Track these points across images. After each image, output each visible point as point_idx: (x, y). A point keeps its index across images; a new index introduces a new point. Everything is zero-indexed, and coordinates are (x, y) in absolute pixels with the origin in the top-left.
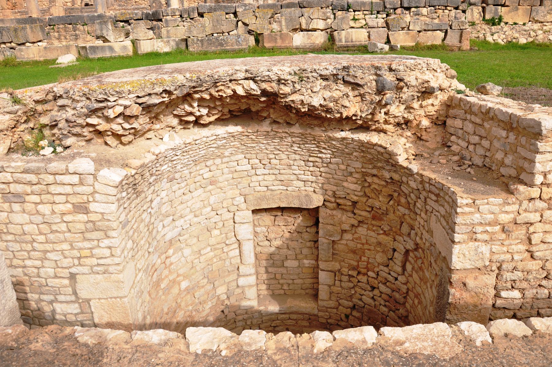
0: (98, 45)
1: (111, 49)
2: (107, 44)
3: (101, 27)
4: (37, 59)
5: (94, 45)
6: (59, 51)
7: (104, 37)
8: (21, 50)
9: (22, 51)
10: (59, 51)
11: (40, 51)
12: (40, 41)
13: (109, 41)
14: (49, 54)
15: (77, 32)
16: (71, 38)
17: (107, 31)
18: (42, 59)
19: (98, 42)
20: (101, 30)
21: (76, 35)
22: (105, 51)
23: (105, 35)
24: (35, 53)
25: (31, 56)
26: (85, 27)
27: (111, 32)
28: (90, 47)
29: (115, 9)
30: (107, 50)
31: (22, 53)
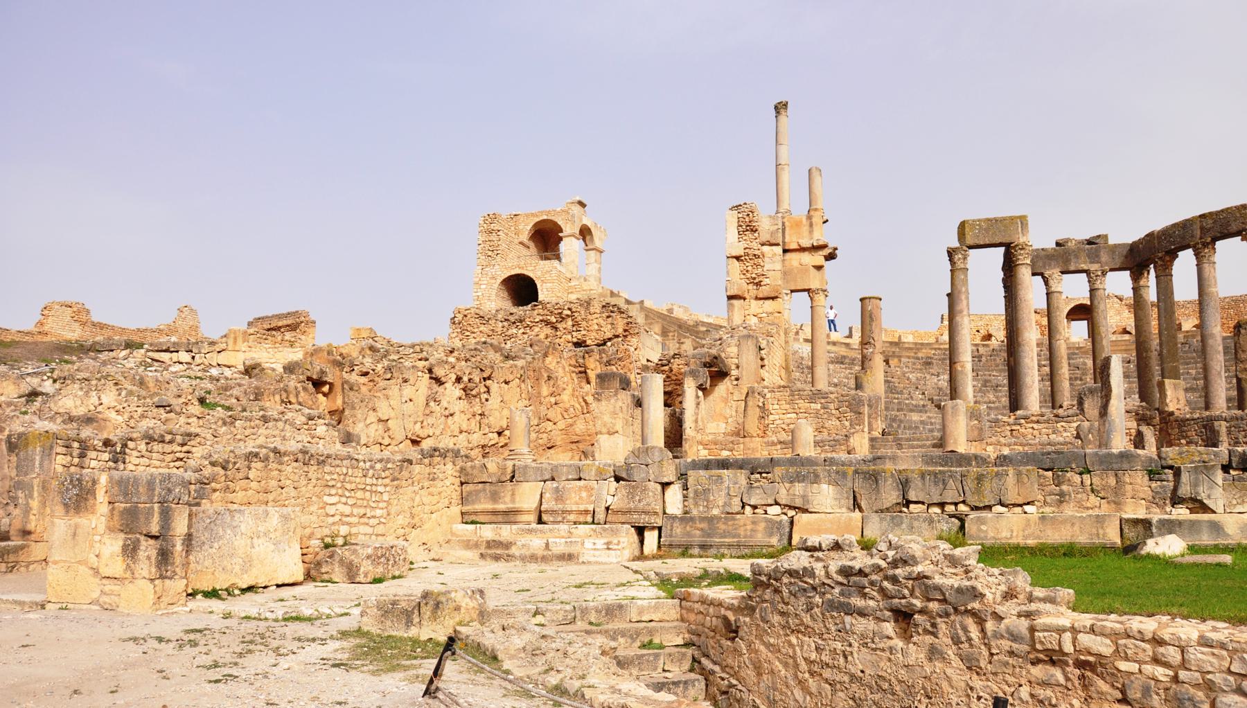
0: (1181, 518)
1: (1216, 527)
2: (1206, 517)
3: (1197, 479)
4: (1019, 540)
5: (1173, 517)
6: (1076, 528)
7: (1201, 502)
8: (981, 521)
9: (983, 524)
10: (1076, 528)
11: (1028, 524)
12: (1028, 504)
13: (1205, 509)
14: (1049, 532)
15: (1064, 488)
16: (1048, 499)
17: (1211, 488)
18: (1031, 542)
19: (1181, 511)
20: (1195, 485)
21: (1062, 494)
22: (1199, 532)
23: (1203, 496)
24: (1015, 528)
25: (1005, 534)
26: (1086, 477)
27: (1218, 492)
28: (1161, 522)
29: (999, 443)
30: (1205, 530)
31: (984, 528)
